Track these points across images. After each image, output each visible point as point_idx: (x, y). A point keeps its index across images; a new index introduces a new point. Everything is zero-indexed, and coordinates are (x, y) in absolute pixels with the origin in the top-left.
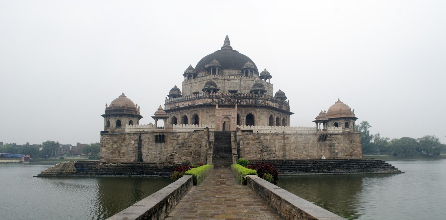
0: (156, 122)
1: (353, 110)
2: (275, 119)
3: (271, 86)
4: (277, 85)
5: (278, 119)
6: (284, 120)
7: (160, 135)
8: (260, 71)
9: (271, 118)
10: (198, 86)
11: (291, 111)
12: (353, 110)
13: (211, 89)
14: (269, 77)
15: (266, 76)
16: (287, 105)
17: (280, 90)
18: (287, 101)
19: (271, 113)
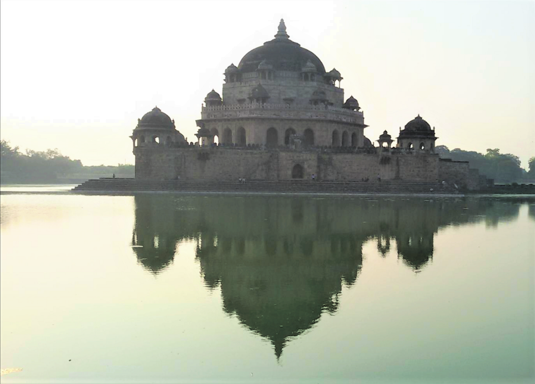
0: (199, 140)
1: (434, 128)
2: (341, 136)
3: (341, 91)
4: (349, 87)
5: (345, 134)
6: (354, 136)
7: (204, 153)
8: (328, 70)
9: (335, 133)
10: (245, 90)
11: (365, 123)
12: (434, 128)
13: (261, 97)
14: (340, 79)
15: (336, 75)
16: (361, 116)
17: (352, 97)
18: (360, 110)
19: (335, 127)
